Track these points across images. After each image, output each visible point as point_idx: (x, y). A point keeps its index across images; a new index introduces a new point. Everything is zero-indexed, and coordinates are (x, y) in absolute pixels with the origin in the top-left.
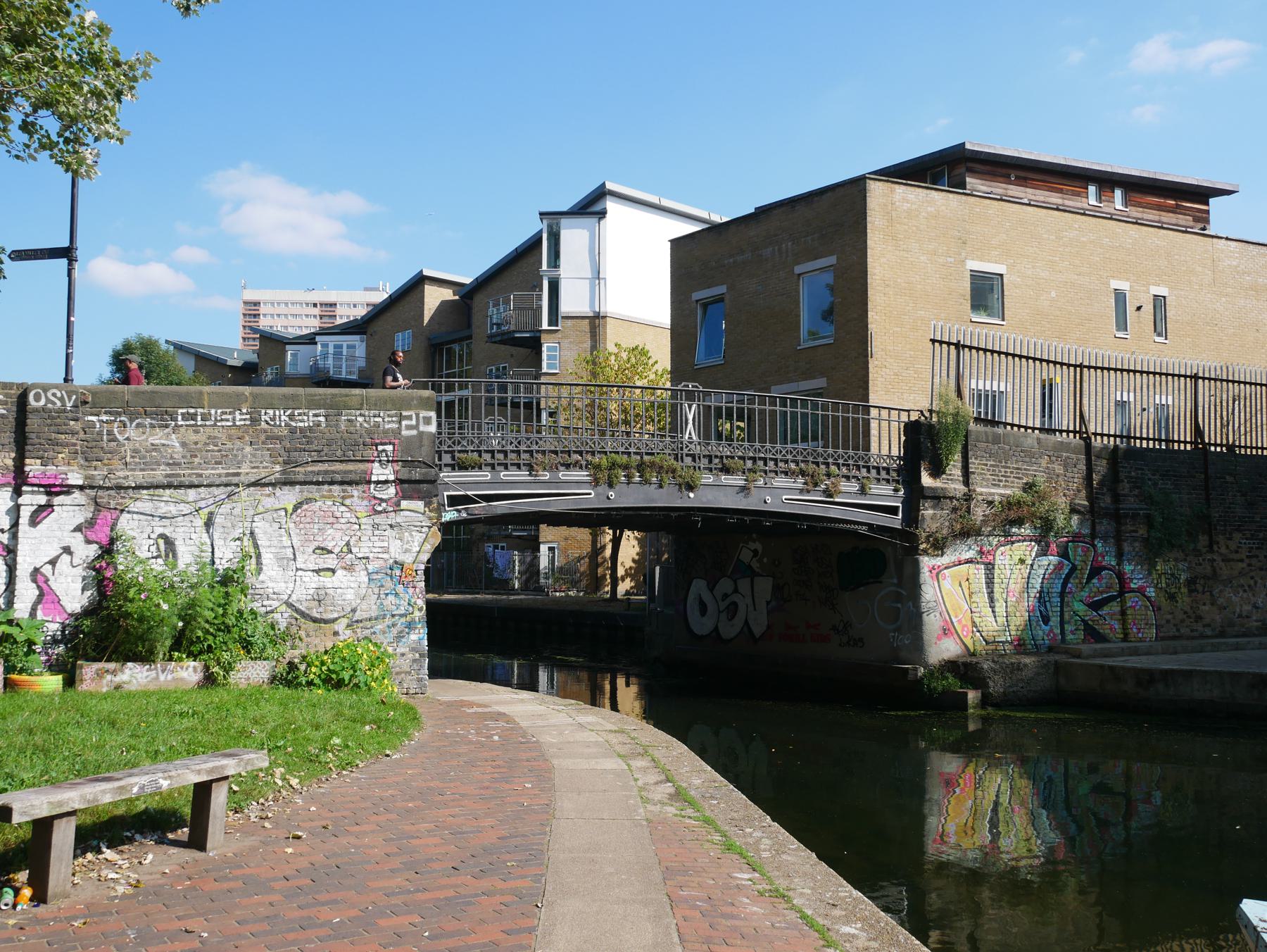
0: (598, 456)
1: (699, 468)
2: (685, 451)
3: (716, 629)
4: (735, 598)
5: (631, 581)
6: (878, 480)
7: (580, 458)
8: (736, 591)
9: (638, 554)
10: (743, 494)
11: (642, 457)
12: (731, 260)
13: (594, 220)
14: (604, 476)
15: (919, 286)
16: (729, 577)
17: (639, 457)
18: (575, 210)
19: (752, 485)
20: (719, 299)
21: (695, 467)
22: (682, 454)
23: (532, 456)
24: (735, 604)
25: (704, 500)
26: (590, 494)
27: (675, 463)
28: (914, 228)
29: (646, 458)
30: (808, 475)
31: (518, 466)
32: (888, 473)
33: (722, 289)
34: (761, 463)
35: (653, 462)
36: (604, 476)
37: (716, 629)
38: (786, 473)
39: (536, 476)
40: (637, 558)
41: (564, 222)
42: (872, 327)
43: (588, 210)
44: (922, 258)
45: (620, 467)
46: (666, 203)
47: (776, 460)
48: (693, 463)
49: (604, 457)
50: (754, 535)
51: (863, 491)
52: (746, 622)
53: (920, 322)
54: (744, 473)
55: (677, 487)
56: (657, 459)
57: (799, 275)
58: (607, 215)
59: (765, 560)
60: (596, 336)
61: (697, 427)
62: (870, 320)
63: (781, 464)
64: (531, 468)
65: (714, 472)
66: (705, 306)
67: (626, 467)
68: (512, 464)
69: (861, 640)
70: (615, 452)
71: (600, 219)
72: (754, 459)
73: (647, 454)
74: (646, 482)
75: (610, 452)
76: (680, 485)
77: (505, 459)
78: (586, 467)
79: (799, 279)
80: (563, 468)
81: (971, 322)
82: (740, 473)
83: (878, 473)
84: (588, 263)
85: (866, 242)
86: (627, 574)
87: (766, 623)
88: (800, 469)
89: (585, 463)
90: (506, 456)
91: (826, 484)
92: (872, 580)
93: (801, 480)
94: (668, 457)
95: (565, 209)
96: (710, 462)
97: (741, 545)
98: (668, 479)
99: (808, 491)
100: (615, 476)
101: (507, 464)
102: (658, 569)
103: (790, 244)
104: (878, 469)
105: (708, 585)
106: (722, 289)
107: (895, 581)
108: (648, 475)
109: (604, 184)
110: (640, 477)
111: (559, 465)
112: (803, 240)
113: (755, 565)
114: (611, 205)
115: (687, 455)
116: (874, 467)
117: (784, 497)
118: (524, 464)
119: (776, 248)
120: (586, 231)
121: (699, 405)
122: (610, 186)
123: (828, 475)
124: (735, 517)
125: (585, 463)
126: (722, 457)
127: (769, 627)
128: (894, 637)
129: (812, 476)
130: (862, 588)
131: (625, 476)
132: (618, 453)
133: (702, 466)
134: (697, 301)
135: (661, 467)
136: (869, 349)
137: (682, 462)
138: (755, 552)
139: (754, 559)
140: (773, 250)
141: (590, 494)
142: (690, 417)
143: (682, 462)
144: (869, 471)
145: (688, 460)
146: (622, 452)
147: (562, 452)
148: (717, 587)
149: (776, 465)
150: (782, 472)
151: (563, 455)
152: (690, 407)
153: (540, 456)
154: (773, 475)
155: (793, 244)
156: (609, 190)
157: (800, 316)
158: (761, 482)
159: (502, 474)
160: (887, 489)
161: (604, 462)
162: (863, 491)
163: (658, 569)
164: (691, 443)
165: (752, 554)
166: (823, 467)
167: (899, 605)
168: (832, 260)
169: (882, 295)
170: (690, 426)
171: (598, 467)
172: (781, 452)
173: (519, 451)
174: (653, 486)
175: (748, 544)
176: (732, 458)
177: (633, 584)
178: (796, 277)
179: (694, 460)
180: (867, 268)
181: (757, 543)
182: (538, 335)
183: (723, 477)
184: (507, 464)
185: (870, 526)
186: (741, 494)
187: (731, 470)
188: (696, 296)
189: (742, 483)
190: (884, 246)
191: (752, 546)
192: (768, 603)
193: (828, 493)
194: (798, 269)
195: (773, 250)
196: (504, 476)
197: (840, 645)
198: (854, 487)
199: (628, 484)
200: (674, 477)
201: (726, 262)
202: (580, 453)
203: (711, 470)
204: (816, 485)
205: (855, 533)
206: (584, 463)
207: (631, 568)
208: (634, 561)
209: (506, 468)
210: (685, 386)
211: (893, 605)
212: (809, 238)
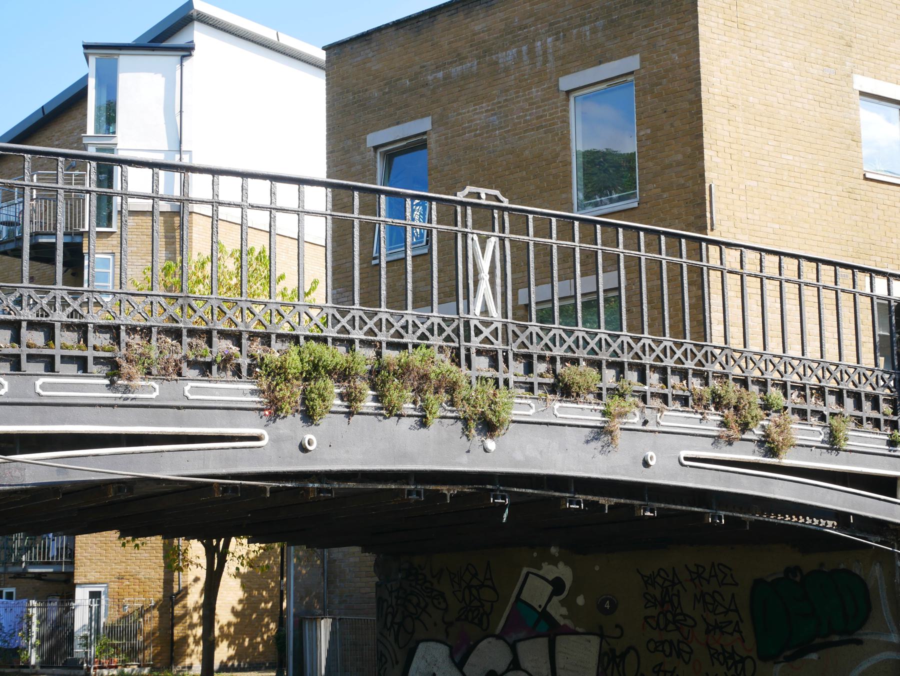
0: (276, 345)
1: (506, 382)
2: (476, 342)
5: (229, 646)
6: (859, 421)
7: (235, 349)
9: (240, 601)
10: (597, 444)
11: (379, 354)
12: (440, 75)
13: (170, 61)
14: (292, 393)
15: (782, 112)
16: (498, 637)
17: (371, 353)
18: (145, 42)
19: (617, 424)
20: (418, 144)
21: (497, 381)
22: (468, 350)
23: (117, 339)
25: (519, 456)
26: (257, 438)
27: (454, 368)
28: (772, 12)
29: (389, 355)
30: (728, 406)
31: (82, 363)
32: (876, 407)
33: (424, 125)
34: (632, 376)
35: (407, 364)
36: (292, 393)
38: (684, 401)
39: (127, 389)
40: (239, 607)
41: (125, 60)
42: (710, 176)
43: (164, 44)
44: (785, 64)
45: (329, 373)
46: (287, 41)
47: (663, 371)
48: (492, 373)
49: (294, 349)
50: (554, 550)
51: (833, 443)
53: (786, 173)
54: (599, 396)
55: (460, 425)
56: (415, 358)
57: (568, 93)
58: (195, 53)
59: (580, 601)
60: (174, 243)
61: (499, 289)
62: (707, 164)
63: (673, 380)
64: (113, 368)
65: (538, 392)
66: (389, 158)
67: (343, 375)
68: (66, 359)
70: (317, 339)
71: (183, 57)
72: (619, 367)
73: (391, 346)
74: (390, 411)
75: (307, 338)
76: (465, 421)
77: (47, 345)
78: (250, 372)
79: (568, 100)
80: (194, 373)
81: (866, 179)
82: (590, 397)
83: (858, 406)
84: (163, 127)
85: (696, 28)
86: (224, 636)
88: (713, 392)
89: (248, 361)
90: (50, 337)
91: (763, 426)
92: (836, 638)
93: (713, 417)
94: (439, 357)
95: (129, 40)
96: (529, 369)
97: (525, 570)
98: (438, 404)
99: (730, 443)
100: (321, 395)
101: (52, 357)
102: (325, 627)
103: (549, 40)
104: (856, 397)
105: (452, 656)
106: (424, 125)
108: (395, 395)
109: (189, 5)
110: (376, 399)
111: (184, 366)
112: (575, 31)
113: (557, 611)
114: (199, 35)
115: (479, 352)
116: (850, 394)
117: (683, 454)
118: (97, 360)
119: (524, 48)
120: (159, 76)
121: (502, 240)
122: (200, 5)
123: (767, 407)
124: (581, 497)
125: (248, 361)
126: (553, 360)
129: (736, 408)
130: (814, 656)
131: (341, 396)
132: (324, 340)
133: (512, 379)
134: (376, 148)
135: (425, 377)
136: (708, 215)
137: (470, 367)
138: (558, 585)
139: (556, 599)
140: (519, 52)
141: (257, 438)
142: (485, 265)
143: (470, 367)
144: (840, 402)
145: (480, 363)
146: (335, 340)
147: (192, 333)
148: (472, 659)
149: (664, 381)
150: (676, 398)
151: (194, 341)
152: (483, 241)
153: (136, 340)
154: (657, 403)
155: (557, 40)
156: (199, 13)
157: (570, 163)
158: (635, 421)
159: (40, 381)
160: (876, 441)
161: (294, 362)
162: (833, 443)
163: (325, 627)
164: (487, 324)
165: (550, 588)
166: (755, 389)
168: (632, 63)
169: (726, 122)
170: (485, 285)
171: (279, 372)
172: (673, 353)
173: (85, 325)
174: (407, 422)
175: (540, 568)
176: (575, 361)
177: (232, 652)
178: (562, 96)
179: (494, 364)
180: (699, 73)
181: (561, 565)
182: (77, 239)
183: (557, 405)
184: (52, 357)
185: (841, 517)
186: (594, 444)
187: (575, 388)
188: (375, 138)
189: (596, 419)
190: (726, 38)
191: (551, 571)
193: (769, 446)
194: (566, 83)
195: (519, 52)
196: (43, 387)
198: (815, 434)
199: (349, 414)
200: (452, 403)
201: (430, 78)
202: (236, 338)
203: (530, 388)
204: (745, 427)
205: (819, 535)
206: (244, 362)
207: (229, 624)
208: (234, 612)
209: (50, 367)
210: (470, 194)
212: (587, 28)
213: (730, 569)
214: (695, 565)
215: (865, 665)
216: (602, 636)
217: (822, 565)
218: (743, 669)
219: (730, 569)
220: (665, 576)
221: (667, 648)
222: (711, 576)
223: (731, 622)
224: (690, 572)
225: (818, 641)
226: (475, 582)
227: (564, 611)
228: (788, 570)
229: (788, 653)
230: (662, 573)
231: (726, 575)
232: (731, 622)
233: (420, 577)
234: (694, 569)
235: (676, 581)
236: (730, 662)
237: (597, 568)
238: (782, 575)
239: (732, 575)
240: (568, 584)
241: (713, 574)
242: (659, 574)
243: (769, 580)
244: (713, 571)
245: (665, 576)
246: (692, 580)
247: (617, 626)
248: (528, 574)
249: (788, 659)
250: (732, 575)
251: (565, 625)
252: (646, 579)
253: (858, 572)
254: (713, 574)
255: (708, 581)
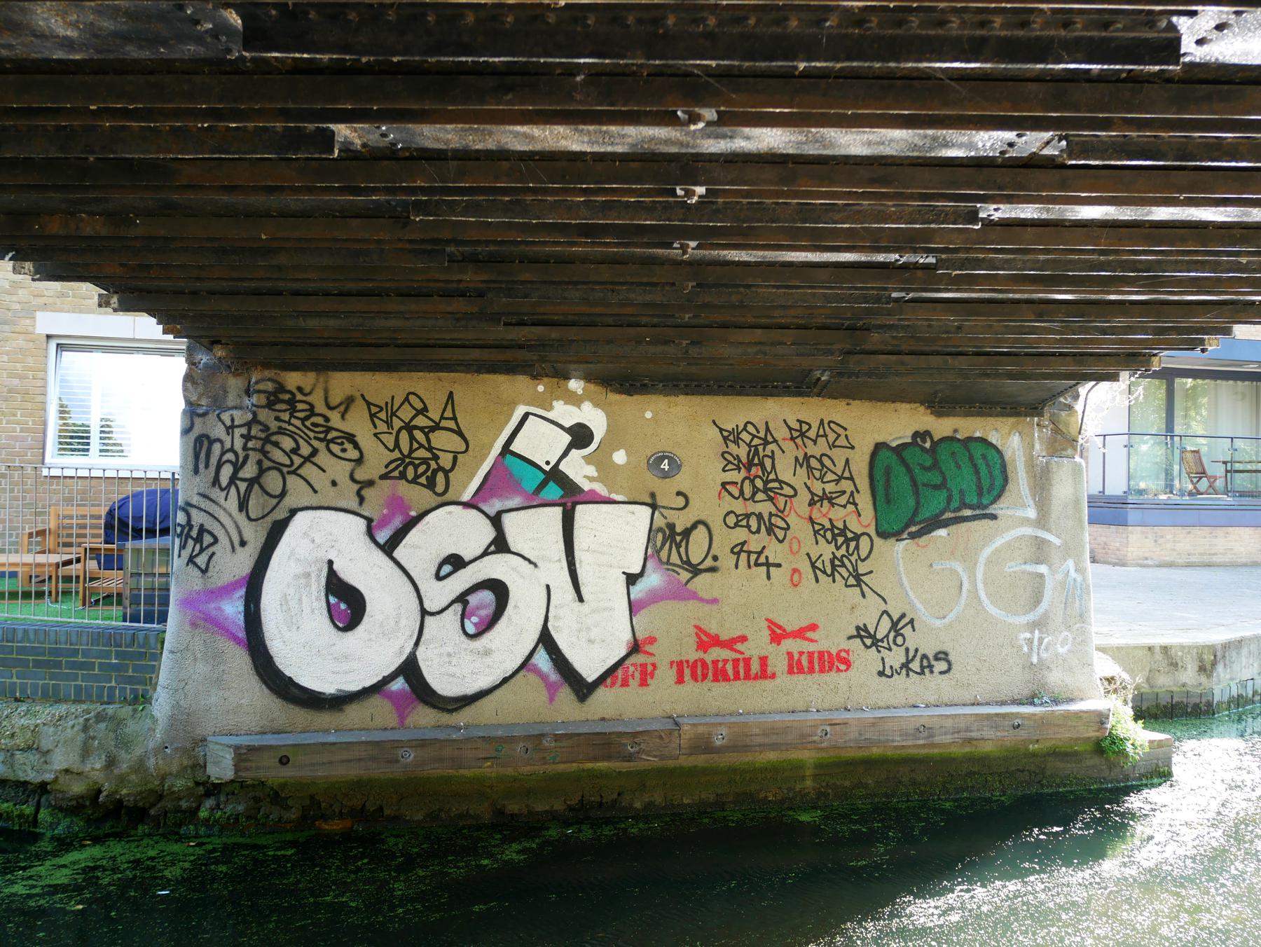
3: (410, 669)
4: (496, 567)
8: (500, 545)
24: (499, 590)
37: (410, 669)
52: (546, 639)
69: (942, 656)
87: (628, 636)
92: (968, 513)
97: (520, 411)
107: (1031, 513)
113: (578, 468)
127: (635, 647)
128: (1030, 642)
130: (942, 532)
138: (580, 436)
139: (575, 453)
165: (567, 439)
167: (1043, 569)
175: (549, 408)
181: (587, 406)
191: (567, 414)
192: (631, 579)
197: (881, 674)
211: (1030, 568)
213: (846, 429)
214: (798, 420)
215: (999, 542)
216: (654, 507)
217: (956, 431)
218: (857, 547)
219: (846, 429)
220: (754, 432)
221: (754, 523)
222: (818, 436)
223: (844, 492)
224: (790, 429)
225: (948, 515)
226: (421, 421)
227: (591, 471)
228: (916, 435)
229: (913, 529)
230: (750, 428)
231: (839, 435)
232: (844, 492)
233: (300, 406)
234: (796, 426)
235: (770, 439)
236: (840, 540)
237: (648, 415)
238: (909, 440)
239: (846, 436)
240: (598, 435)
241: (821, 432)
242: (745, 429)
243: (894, 444)
244: (821, 430)
245: (754, 432)
246: (792, 439)
247: (679, 493)
248: (526, 416)
249: (913, 536)
250: (846, 436)
251: (592, 491)
252: (726, 434)
253: (994, 442)
254: (821, 432)
255: (815, 442)
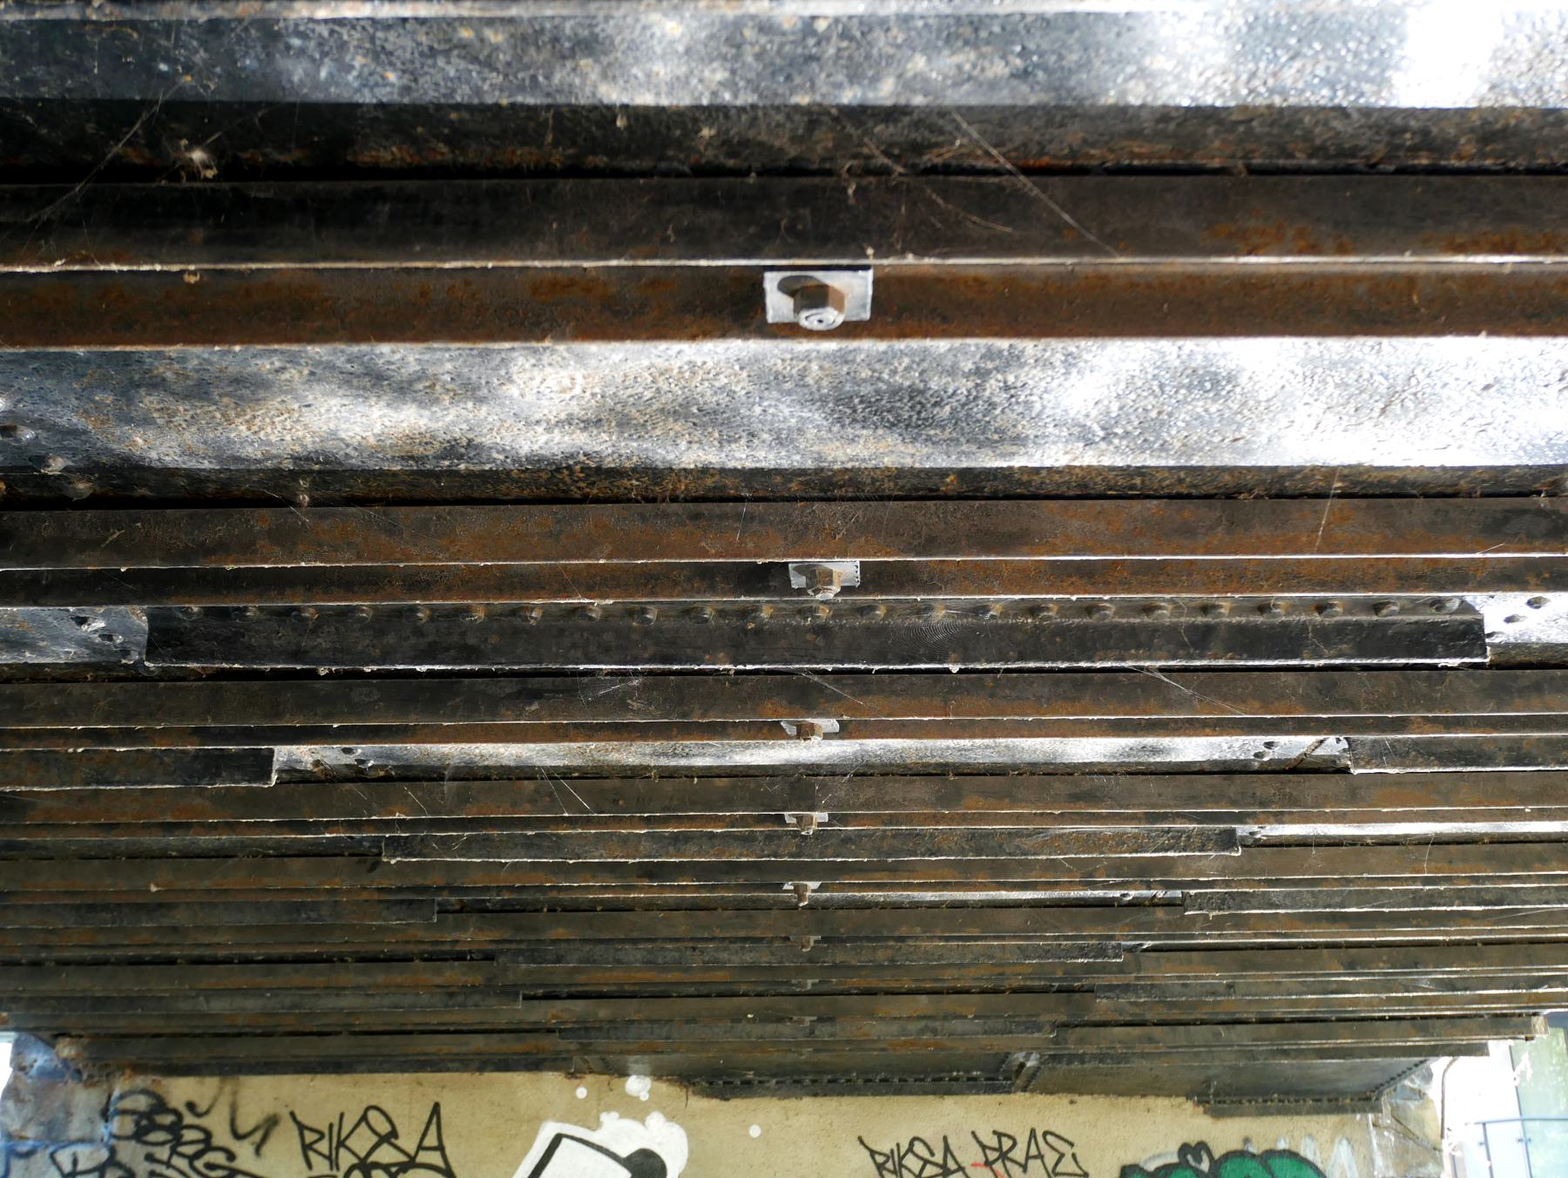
175: (595, 1125)
181: (656, 1120)
213: (1072, 1145)
214: (995, 1132)
217: (1247, 1140)
219: (1072, 1145)
220: (926, 1155)
222: (1028, 1157)
224: (984, 1147)
226: (386, 1155)
228: (1184, 1149)
230: (919, 1147)
231: (1062, 1156)
233: (189, 1135)
234: (993, 1142)
235: (952, 1165)
237: (755, 1131)
238: (1174, 1159)
239: (1074, 1156)
241: (1033, 1151)
242: (910, 1149)
243: (1151, 1167)
244: (1033, 1147)
245: (926, 1155)
246: (988, 1164)
250: (1074, 1156)
252: (880, 1159)
253: (1310, 1157)
254: (1033, 1151)
255: (1025, 1168)
